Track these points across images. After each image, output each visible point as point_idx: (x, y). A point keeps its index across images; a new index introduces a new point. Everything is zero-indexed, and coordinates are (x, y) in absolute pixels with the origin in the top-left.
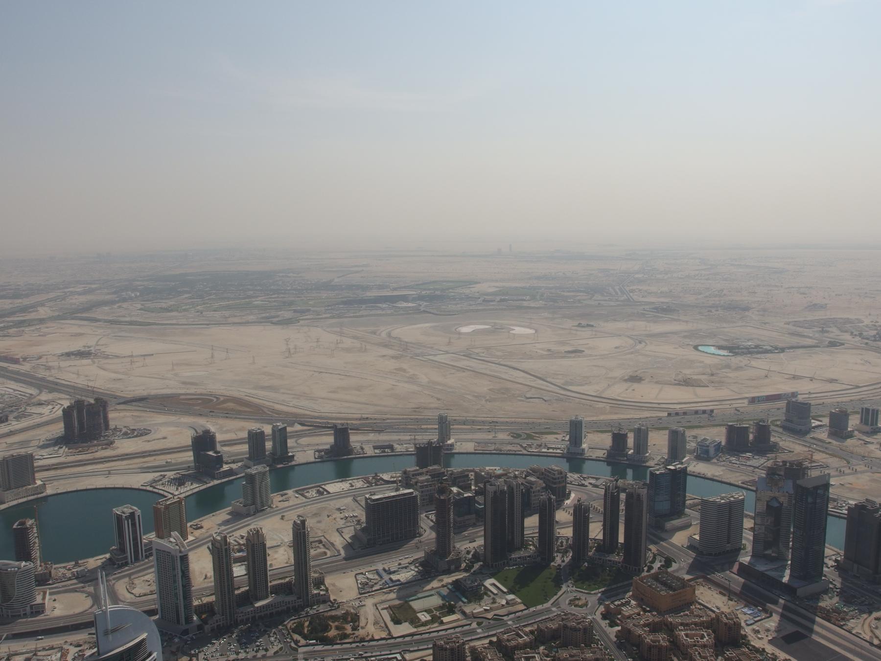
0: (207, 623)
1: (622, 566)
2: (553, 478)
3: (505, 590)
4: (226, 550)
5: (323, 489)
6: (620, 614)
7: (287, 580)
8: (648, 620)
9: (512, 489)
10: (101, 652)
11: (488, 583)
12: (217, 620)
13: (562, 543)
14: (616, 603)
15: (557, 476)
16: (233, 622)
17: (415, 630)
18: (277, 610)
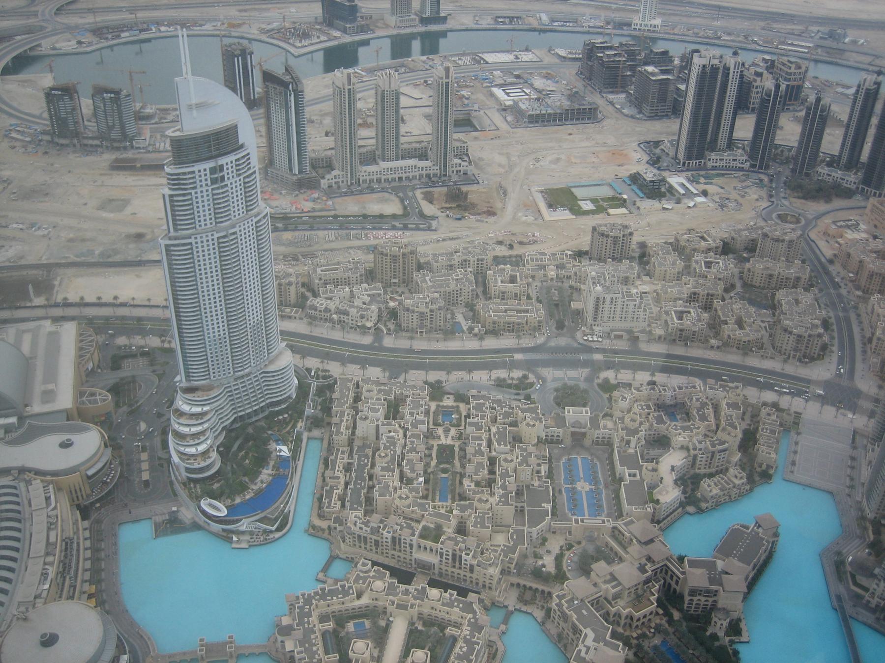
0: (323, 178)
1: (858, 188)
2: (787, 73)
3: (695, 192)
4: (349, 90)
5: (480, 57)
6: (841, 236)
7: (423, 145)
8: (877, 246)
9: (729, 69)
10: (184, 129)
11: (676, 180)
12: (335, 176)
13: (782, 151)
14: (839, 224)
15: (793, 70)
16: (354, 181)
17: (574, 217)
18: (408, 174)
